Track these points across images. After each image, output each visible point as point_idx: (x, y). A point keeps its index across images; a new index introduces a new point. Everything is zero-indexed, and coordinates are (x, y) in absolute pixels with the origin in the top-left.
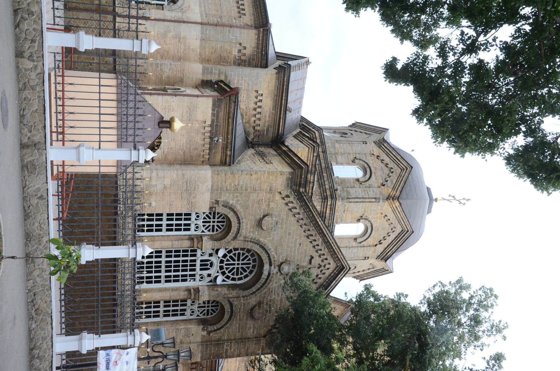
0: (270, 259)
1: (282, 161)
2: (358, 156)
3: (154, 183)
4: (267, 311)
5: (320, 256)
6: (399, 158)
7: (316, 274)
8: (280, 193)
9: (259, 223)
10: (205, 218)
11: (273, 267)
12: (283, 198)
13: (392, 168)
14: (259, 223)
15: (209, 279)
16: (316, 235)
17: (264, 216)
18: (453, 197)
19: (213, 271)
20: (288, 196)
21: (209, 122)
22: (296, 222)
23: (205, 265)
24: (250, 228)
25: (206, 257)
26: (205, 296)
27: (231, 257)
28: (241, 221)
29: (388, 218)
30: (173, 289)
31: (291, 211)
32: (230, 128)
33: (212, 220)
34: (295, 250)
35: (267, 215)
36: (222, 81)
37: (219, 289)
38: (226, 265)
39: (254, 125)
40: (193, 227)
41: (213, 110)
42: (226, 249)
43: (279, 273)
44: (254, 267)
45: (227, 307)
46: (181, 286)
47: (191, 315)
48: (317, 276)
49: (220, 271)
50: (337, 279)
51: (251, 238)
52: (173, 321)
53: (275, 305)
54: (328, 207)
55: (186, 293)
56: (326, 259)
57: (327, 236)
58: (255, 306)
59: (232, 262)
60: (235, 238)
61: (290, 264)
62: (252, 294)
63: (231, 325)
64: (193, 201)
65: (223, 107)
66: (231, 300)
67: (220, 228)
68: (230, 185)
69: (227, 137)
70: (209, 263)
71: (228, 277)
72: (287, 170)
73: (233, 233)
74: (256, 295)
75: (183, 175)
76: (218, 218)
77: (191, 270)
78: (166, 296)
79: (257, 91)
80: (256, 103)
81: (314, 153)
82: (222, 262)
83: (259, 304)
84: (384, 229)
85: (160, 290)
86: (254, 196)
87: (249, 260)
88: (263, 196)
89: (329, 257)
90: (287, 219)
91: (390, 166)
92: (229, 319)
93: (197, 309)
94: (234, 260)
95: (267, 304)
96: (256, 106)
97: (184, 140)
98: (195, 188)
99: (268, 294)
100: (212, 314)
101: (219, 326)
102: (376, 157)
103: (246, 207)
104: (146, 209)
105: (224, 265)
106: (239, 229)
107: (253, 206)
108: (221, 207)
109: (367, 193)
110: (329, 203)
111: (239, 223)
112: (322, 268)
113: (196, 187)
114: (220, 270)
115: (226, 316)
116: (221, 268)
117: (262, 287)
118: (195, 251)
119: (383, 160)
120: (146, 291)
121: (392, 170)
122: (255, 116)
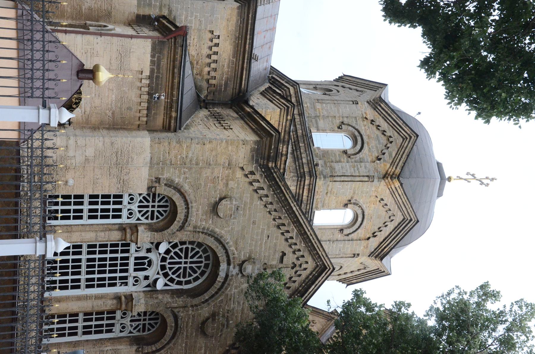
0: (228, 256)
1: (246, 126)
2: (346, 121)
3: (71, 153)
4: (223, 325)
5: (294, 252)
6: (400, 123)
7: (288, 276)
8: (242, 168)
9: (214, 209)
10: (141, 201)
11: (231, 267)
12: (246, 176)
13: (390, 137)
14: (214, 209)
15: (146, 283)
16: (289, 224)
17: (221, 199)
18: (473, 175)
19: (151, 272)
20: (252, 173)
21: (147, 73)
22: (262, 207)
23: (142, 264)
24: (202, 215)
25: (142, 254)
26: (140, 306)
27: (176, 253)
28: (190, 205)
29: (385, 202)
30: (98, 297)
31: (257, 193)
32: (176, 81)
33: (151, 204)
34: (261, 244)
35: (224, 198)
36: (164, 17)
37: (160, 297)
38: (170, 263)
39: (209, 77)
40: (125, 213)
41: (153, 56)
42: (170, 243)
43: (240, 275)
44: (206, 266)
45: (170, 321)
46: (108, 292)
47: (121, 331)
48: (290, 278)
49: (161, 273)
50: (317, 282)
51: (204, 229)
52: (96, 340)
53: (234, 318)
54: (305, 187)
55: (115, 301)
56: (303, 256)
57: (304, 226)
58: (208, 319)
59: (177, 260)
60: (182, 228)
61: (254, 263)
62: (203, 303)
63: (174, 344)
64: (126, 178)
65: (166, 52)
66: (176, 310)
67: (162, 215)
68: (176, 157)
69: (172, 93)
70: (146, 261)
71: (172, 280)
72: (252, 138)
73: (179, 222)
74: (209, 304)
75: (112, 143)
76: (159, 202)
77: (121, 271)
78: (87, 306)
79: (212, 32)
80: (210, 48)
81: (287, 115)
82: (164, 259)
83: (214, 316)
84: (379, 217)
85: (79, 298)
86: (207, 173)
87: (200, 257)
88: (219, 172)
89: (306, 254)
90: (251, 203)
91: (388, 134)
92: (173, 337)
93: (129, 323)
94: (180, 257)
95: (223, 316)
96: (211, 53)
97: (114, 96)
98: (128, 162)
99: (224, 302)
100: (149, 330)
101: (158, 345)
102: (369, 122)
103: (196, 188)
104: (60, 189)
105: (166, 264)
106: (187, 216)
107: (206, 185)
108: (164, 187)
109: (358, 169)
110: (307, 182)
111: (188, 208)
112: (297, 268)
113: (130, 159)
114: (162, 270)
115: (169, 332)
116: (163, 268)
117: (216, 293)
118: (128, 245)
119: (379, 126)
120: (59, 300)
121: (391, 139)
122: (209, 65)
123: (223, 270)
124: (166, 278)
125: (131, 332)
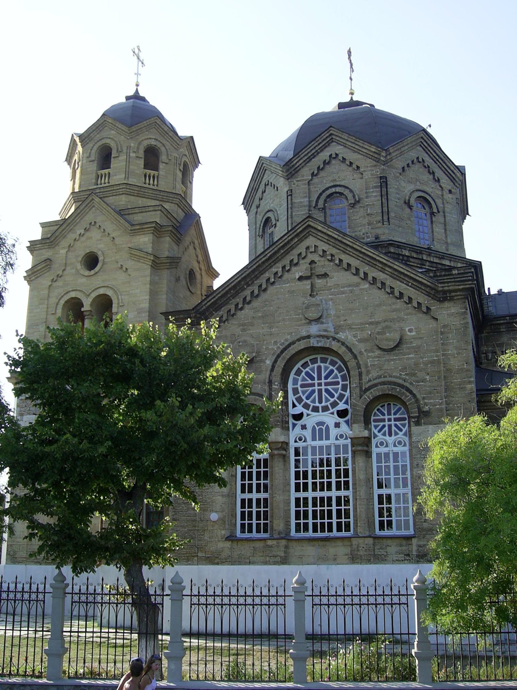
25: (308, 433)
49: (331, 411)
70: (317, 428)
82: (316, 409)
93: (393, 437)
116: (325, 409)
123: (318, 342)
124: (338, 404)
125: (405, 434)
